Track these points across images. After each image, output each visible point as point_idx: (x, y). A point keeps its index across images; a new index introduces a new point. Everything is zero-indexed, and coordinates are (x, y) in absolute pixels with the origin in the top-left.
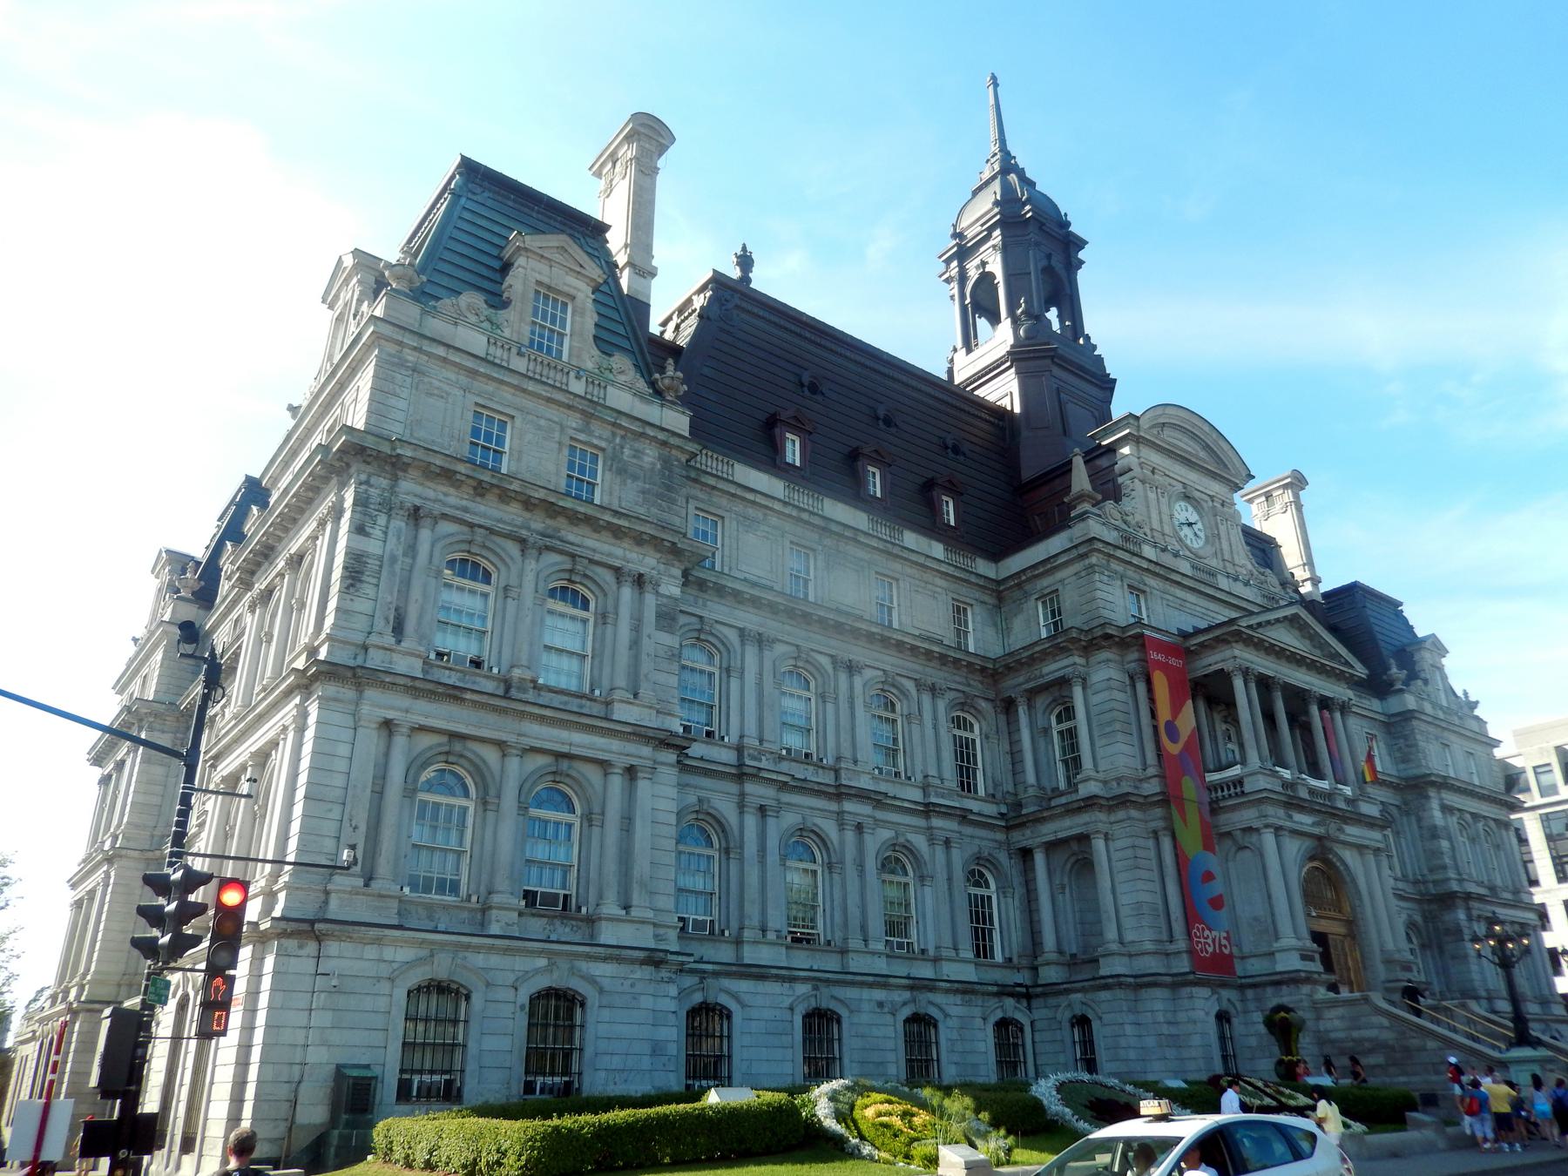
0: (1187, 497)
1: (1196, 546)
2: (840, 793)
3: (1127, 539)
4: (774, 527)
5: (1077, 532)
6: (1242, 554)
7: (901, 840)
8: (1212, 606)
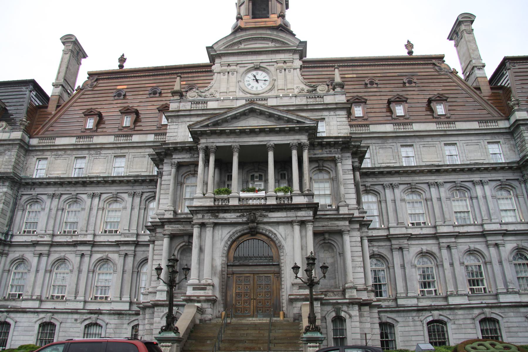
0: (257, 68)
1: (259, 89)
2: (75, 244)
3: (198, 103)
4: (69, 155)
7: (104, 257)
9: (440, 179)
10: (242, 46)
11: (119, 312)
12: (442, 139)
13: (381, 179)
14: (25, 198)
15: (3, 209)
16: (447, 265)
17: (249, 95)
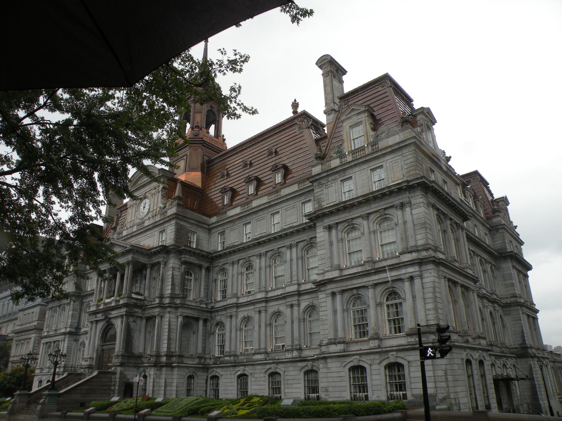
9: (263, 250)
10: (139, 183)
12: (270, 210)
13: (229, 259)
14: (85, 304)
15: (72, 315)
16: (257, 327)
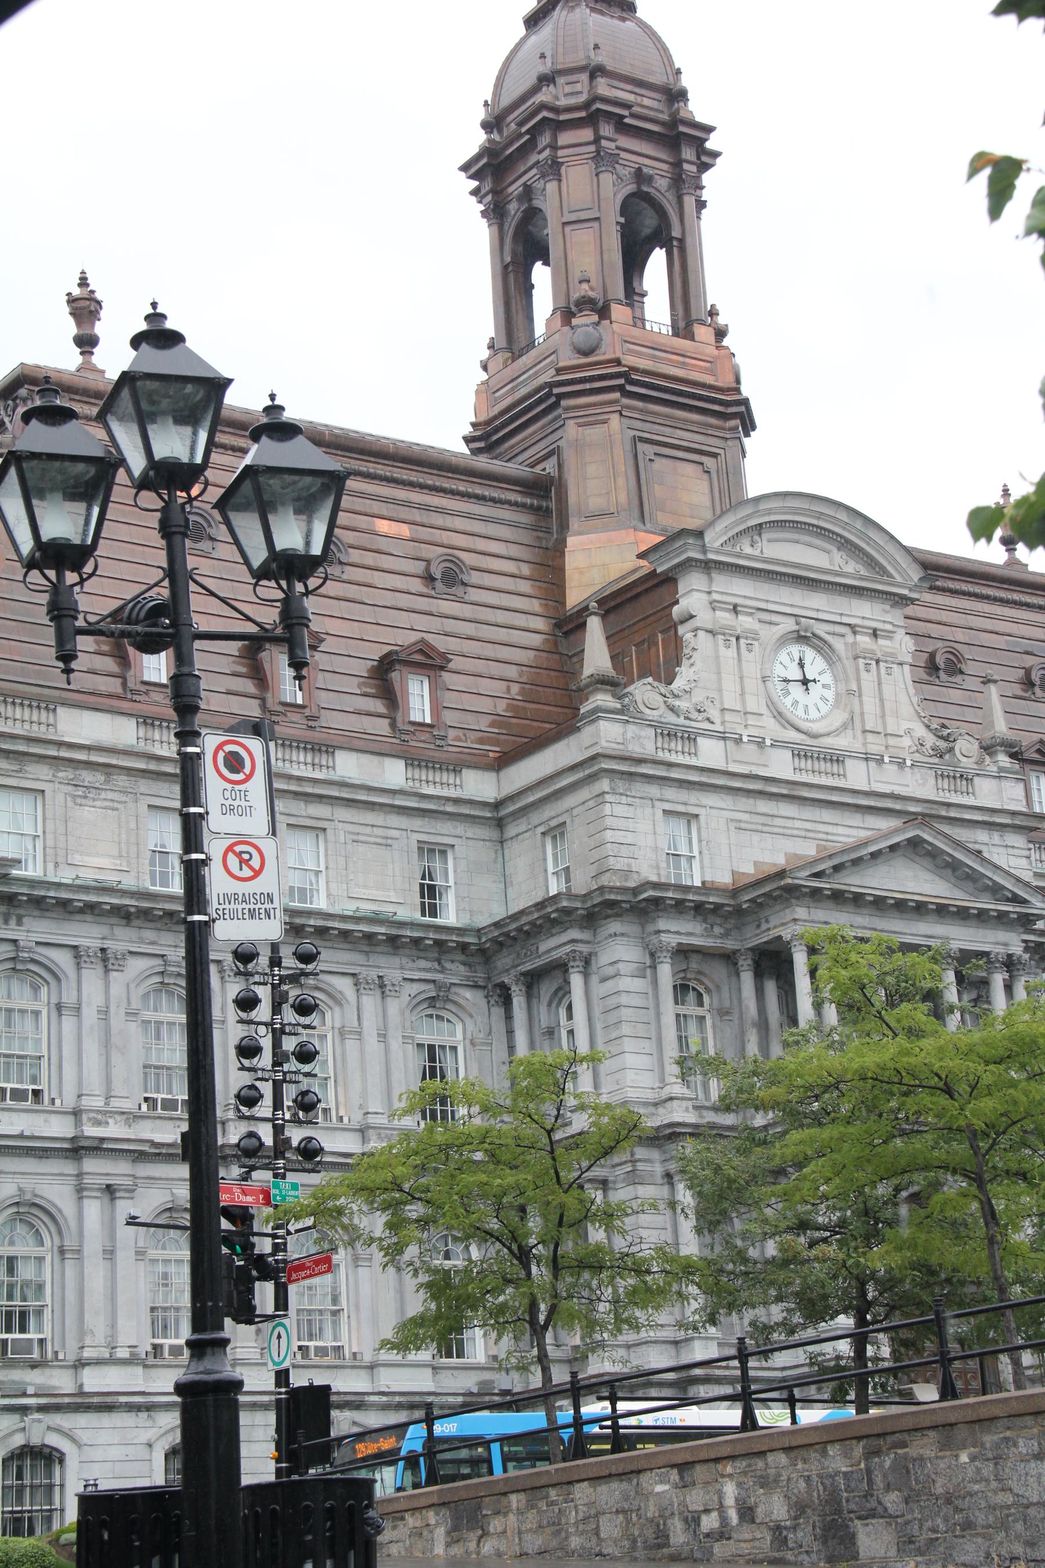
0: (801, 638)
1: (813, 714)
5: (586, 734)
6: (906, 710)
8: (827, 815)
11: (417, 1399)
17: (792, 735)
